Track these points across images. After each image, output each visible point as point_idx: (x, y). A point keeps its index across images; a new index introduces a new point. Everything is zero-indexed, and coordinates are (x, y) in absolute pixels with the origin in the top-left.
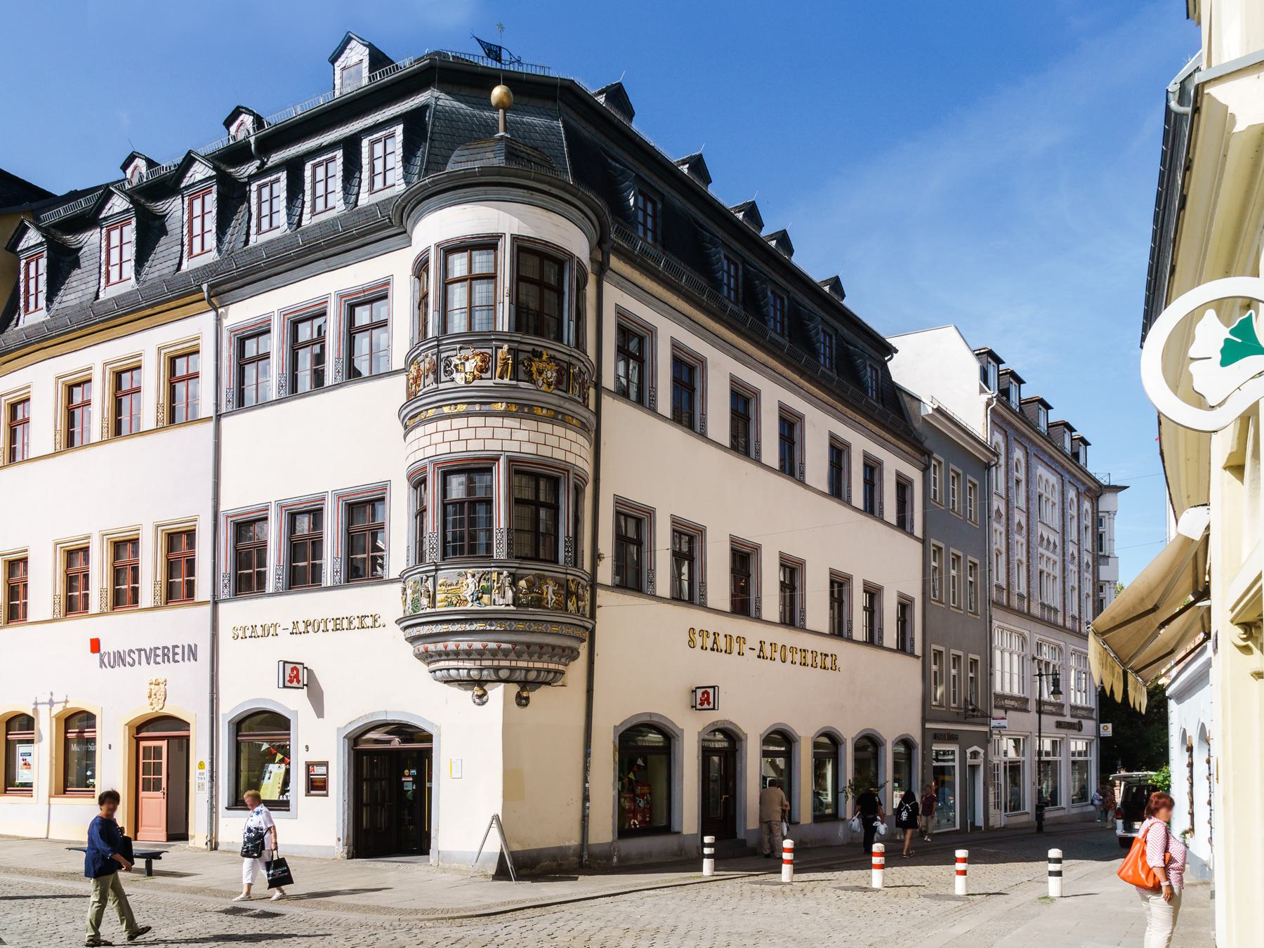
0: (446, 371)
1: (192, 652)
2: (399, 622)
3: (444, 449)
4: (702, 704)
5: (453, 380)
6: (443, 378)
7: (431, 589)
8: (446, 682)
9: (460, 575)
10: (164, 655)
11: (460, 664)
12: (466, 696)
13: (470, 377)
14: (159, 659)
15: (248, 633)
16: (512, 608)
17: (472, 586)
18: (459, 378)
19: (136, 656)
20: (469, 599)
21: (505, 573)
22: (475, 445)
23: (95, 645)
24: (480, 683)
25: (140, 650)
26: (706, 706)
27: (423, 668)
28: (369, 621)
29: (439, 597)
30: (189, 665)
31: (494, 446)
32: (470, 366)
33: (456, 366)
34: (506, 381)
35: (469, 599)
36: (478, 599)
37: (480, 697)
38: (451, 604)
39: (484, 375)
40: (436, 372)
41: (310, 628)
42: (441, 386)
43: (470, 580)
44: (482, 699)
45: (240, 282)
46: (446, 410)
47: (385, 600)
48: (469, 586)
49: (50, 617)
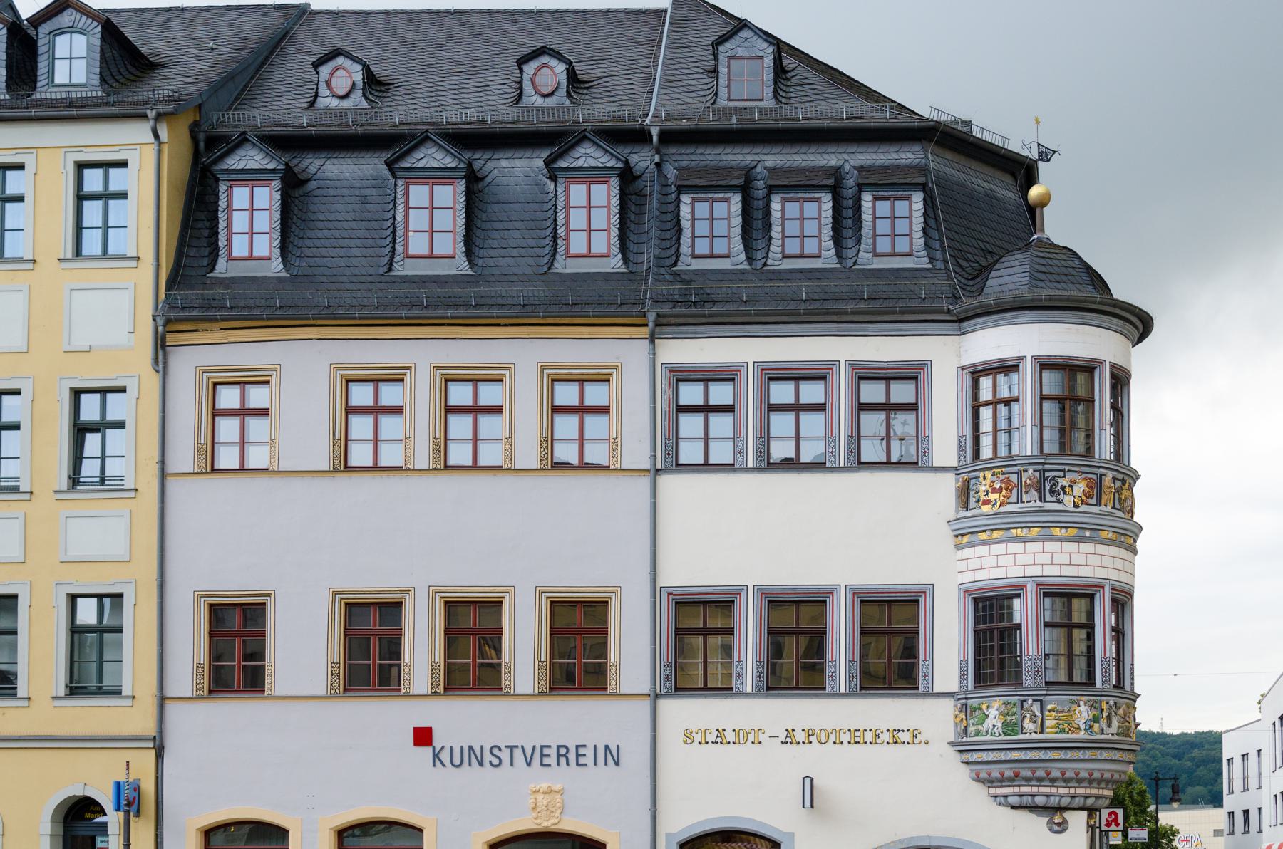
0: (1052, 492)
1: (613, 756)
2: (952, 744)
3: (1054, 571)
4: (1108, 825)
5: (1061, 502)
6: (1048, 497)
7: (1038, 714)
8: (1013, 807)
9: (1071, 702)
10: (559, 755)
11: (1061, 791)
12: (1040, 822)
13: (1078, 502)
14: (552, 761)
15: (711, 738)
16: (1116, 737)
17: (1085, 714)
18: (1068, 500)
19: (505, 755)
20: (1083, 727)
21: (1112, 703)
22: (1085, 572)
23: (423, 737)
24: (1060, 809)
25: (512, 748)
26: (1113, 827)
27: (981, 791)
28: (904, 737)
29: (1048, 723)
30: (606, 772)
31: (1101, 573)
32: (1080, 488)
33: (1063, 488)
34: (1109, 509)
35: (1083, 727)
36: (1091, 727)
37: (1059, 824)
38: (1063, 731)
39: (1090, 501)
40: (1041, 490)
41: (813, 739)
42: (1048, 506)
43: (1083, 708)
44: (1062, 827)
45: (703, 320)
46: (1057, 532)
47: (932, 717)
48: (1083, 713)
49: (323, 693)
